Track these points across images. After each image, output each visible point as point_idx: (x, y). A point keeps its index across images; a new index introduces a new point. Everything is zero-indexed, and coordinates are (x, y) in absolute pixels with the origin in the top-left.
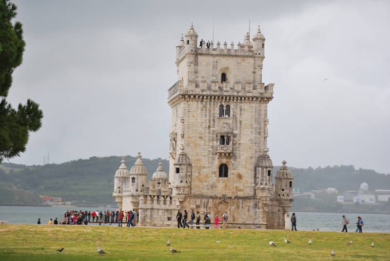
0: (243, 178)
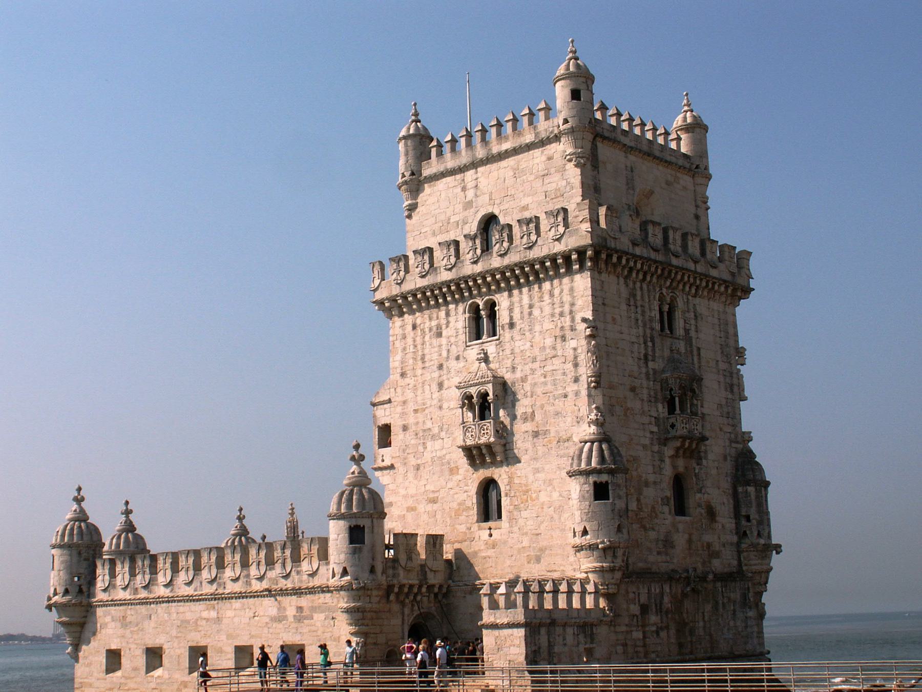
0: (717, 519)
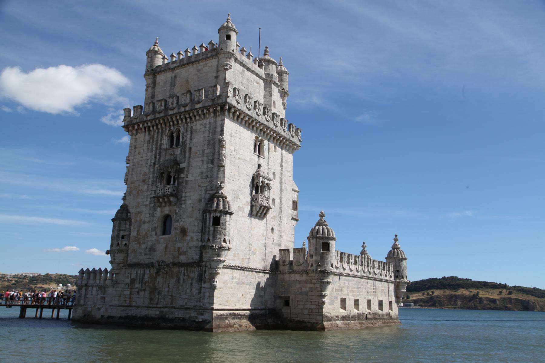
0: (188, 234)
